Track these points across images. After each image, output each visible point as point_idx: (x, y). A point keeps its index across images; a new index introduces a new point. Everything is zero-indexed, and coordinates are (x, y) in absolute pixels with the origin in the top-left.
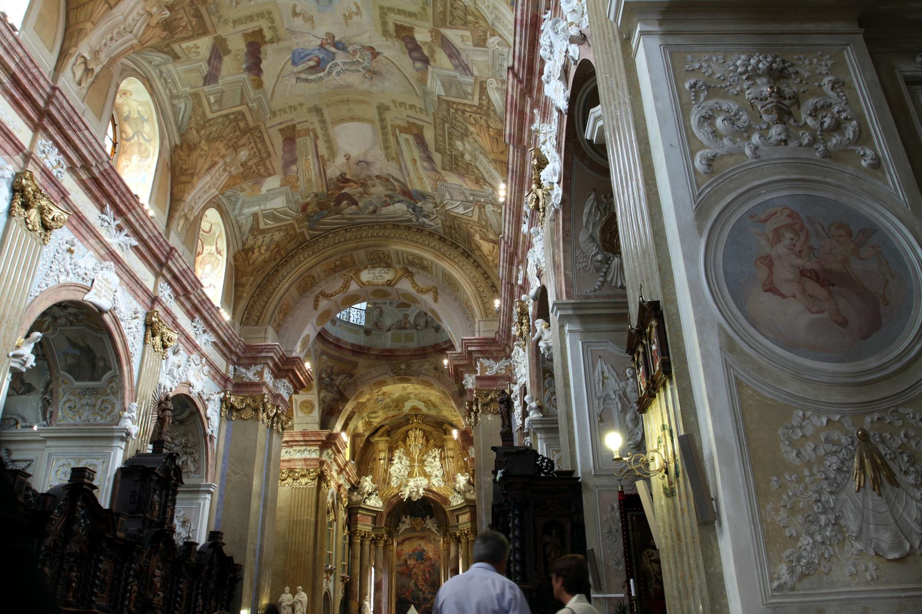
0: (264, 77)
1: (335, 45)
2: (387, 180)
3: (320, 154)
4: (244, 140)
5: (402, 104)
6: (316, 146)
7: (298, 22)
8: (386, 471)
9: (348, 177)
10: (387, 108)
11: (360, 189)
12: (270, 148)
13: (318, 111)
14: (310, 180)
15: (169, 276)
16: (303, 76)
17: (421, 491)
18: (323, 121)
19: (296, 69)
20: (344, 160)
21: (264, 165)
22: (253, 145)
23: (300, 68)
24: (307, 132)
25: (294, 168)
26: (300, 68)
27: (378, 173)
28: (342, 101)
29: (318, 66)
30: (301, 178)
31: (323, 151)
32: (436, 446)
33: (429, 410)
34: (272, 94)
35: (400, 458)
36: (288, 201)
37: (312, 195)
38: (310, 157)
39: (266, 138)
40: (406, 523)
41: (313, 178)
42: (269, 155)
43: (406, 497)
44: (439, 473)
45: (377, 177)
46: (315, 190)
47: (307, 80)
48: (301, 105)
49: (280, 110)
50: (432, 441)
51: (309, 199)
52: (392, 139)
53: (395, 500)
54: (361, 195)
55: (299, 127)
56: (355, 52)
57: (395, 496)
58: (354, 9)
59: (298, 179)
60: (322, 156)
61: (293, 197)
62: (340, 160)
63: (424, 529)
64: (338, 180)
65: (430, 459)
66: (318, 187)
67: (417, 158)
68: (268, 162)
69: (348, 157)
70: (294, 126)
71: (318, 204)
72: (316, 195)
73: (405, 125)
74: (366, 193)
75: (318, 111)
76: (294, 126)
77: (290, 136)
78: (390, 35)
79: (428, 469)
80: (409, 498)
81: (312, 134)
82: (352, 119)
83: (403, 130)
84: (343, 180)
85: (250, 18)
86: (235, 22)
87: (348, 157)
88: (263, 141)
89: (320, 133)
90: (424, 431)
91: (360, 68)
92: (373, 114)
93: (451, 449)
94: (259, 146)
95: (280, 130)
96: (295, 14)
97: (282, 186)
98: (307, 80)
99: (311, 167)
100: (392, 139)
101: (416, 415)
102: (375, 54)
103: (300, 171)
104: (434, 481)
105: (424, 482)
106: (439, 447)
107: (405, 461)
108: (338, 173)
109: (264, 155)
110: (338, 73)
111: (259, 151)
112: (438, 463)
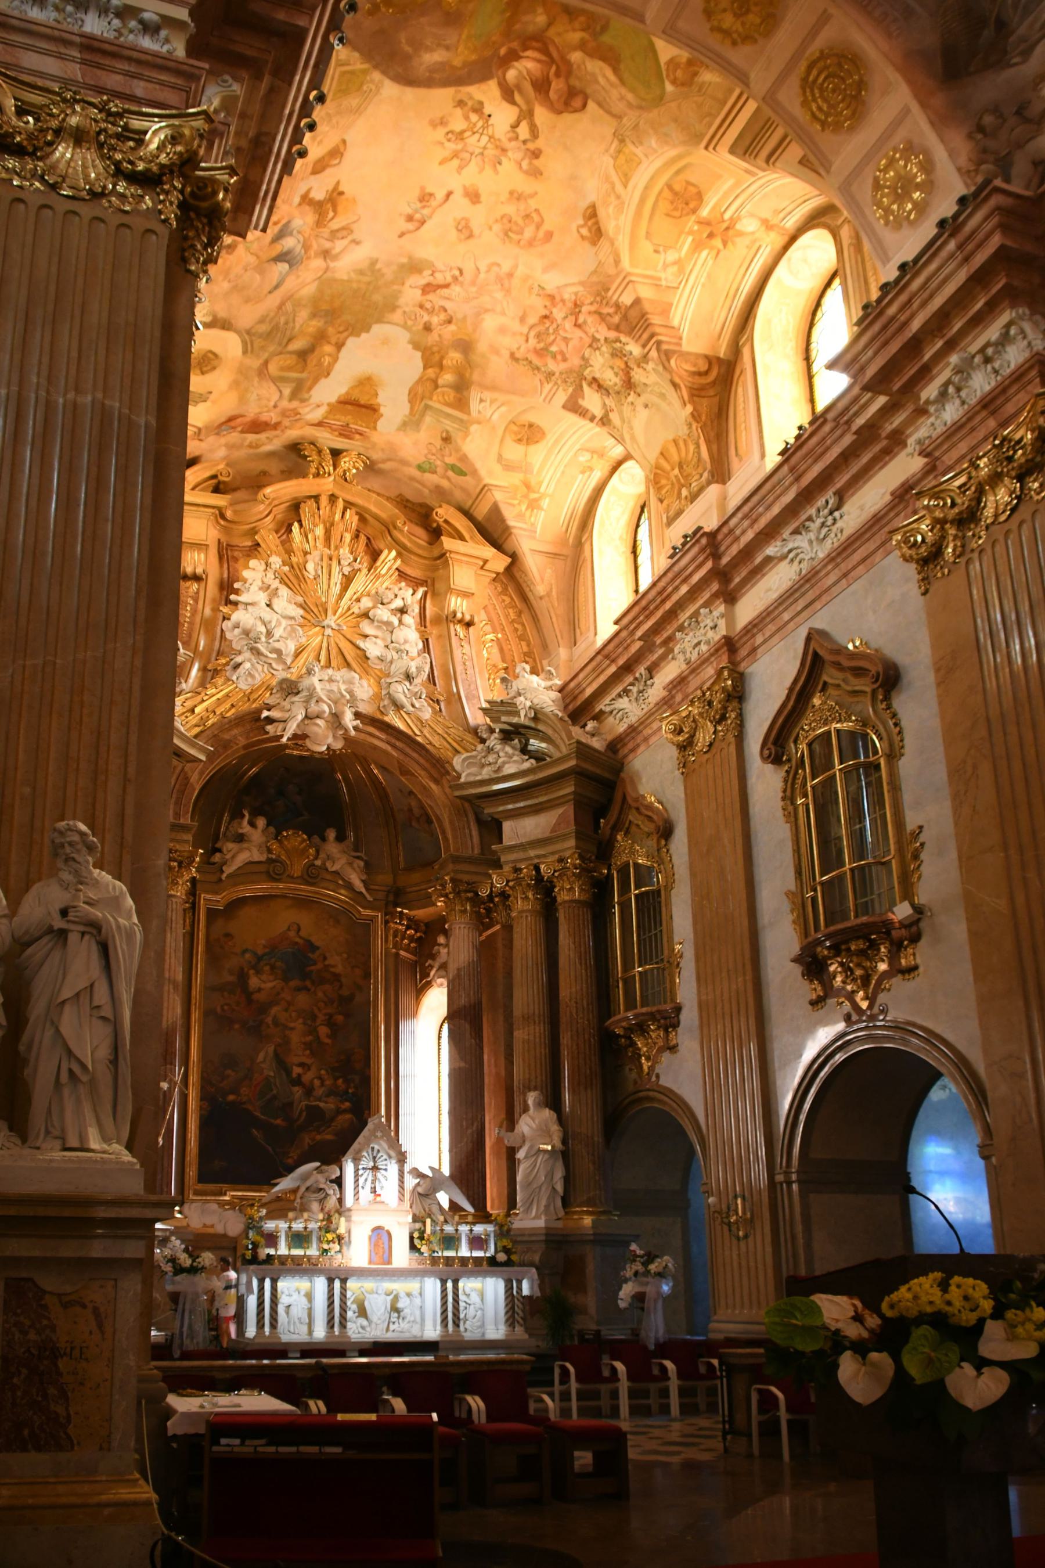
8: (209, 625)
17: (349, 720)
32: (402, 575)
33: (411, 423)
35: (265, 588)
40: (251, 844)
43: (292, 728)
44: (416, 663)
50: (389, 558)
53: (240, 738)
57: (240, 720)
63: (312, 875)
65: (383, 614)
79: (374, 649)
80: (299, 738)
90: (362, 519)
93: (466, 595)
101: (336, 453)
104: (400, 691)
105: (364, 690)
106: (415, 583)
107: (286, 603)
112: (410, 635)
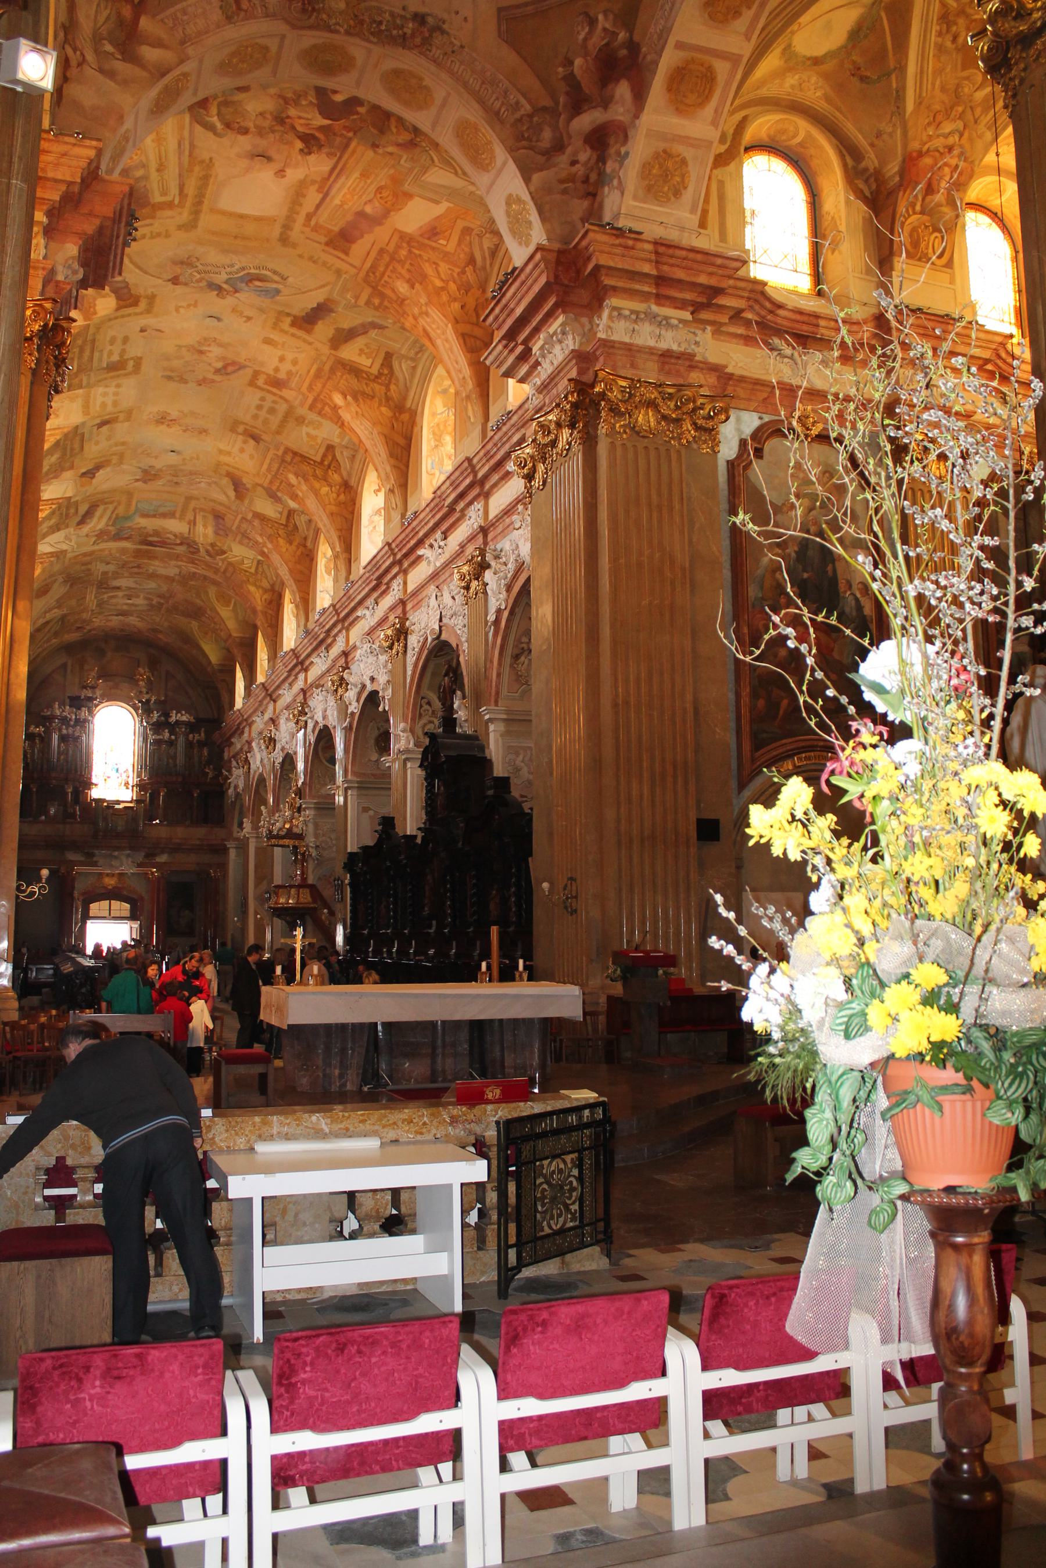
0: (321, 300)
1: (219, 288)
2: (228, 125)
3: (321, 196)
4: (388, 292)
5: (159, 235)
6: (318, 207)
7: (248, 313)
9: (299, 145)
10: (180, 228)
11: (292, 112)
12: (374, 254)
13: (284, 240)
14: (364, 175)
15: (462, 505)
16: (276, 278)
18: (287, 227)
19: (280, 287)
20: (289, 172)
21: (395, 252)
22: (386, 278)
23: (275, 286)
24: (316, 229)
25: (368, 209)
26: (275, 286)
27: (242, 138)
28: (244, 238)
29: (250, 279)
30: (372, 188)
31: (313, 196)
34: (323, 286)
36: (425, 170)
37: (380, 151)
38: (337, 202)
39: (368, 264)
41: (357, 175)
42: (382, 251)
45: (245, 131)
46: (370, 154)
47: (275, 272)
48: (300, 256)
49: (329, 268)
51: (391, 149)
52: (191, 190)
54: (296, 100)
55: (323, 239)
56: (199, 281)
58: (182, 311)
59: (379, 190)
60: (319, 191)
61: (411, 170)
62: (295, 175)
64: (320, 147)
66: (361, 155)
67: (154, 175)
68: (391, 248)
69: (281, 173)
70: (327, 244)
71: (382, 132)
72: (375, 146)
73: (159, 213)
74: (286, 101)
75: (284, 240)
76: (327, 244)
77: (342, 240)
78: (147, 297)
81: (313, 223)
82: (242, 217)
83: (170, 205)
84: (310, 142)
85: (293, 335)
86: (310, 344)
87: (281, 173)
88: (373, 268)
89: (301, 219)
91: (200, 267)
92: (206, 220)
94: (382, 269)
95: (347, 254)
96: (249, 319)
97: (409, 196)
98: (275, 272)
99: (345, 190)
100: (191, 190)
102: (175, 281)
103: (365, 198)
108: (312, 158)
109: (386, 258)
110: (232, 266)
111: (387, 266)
